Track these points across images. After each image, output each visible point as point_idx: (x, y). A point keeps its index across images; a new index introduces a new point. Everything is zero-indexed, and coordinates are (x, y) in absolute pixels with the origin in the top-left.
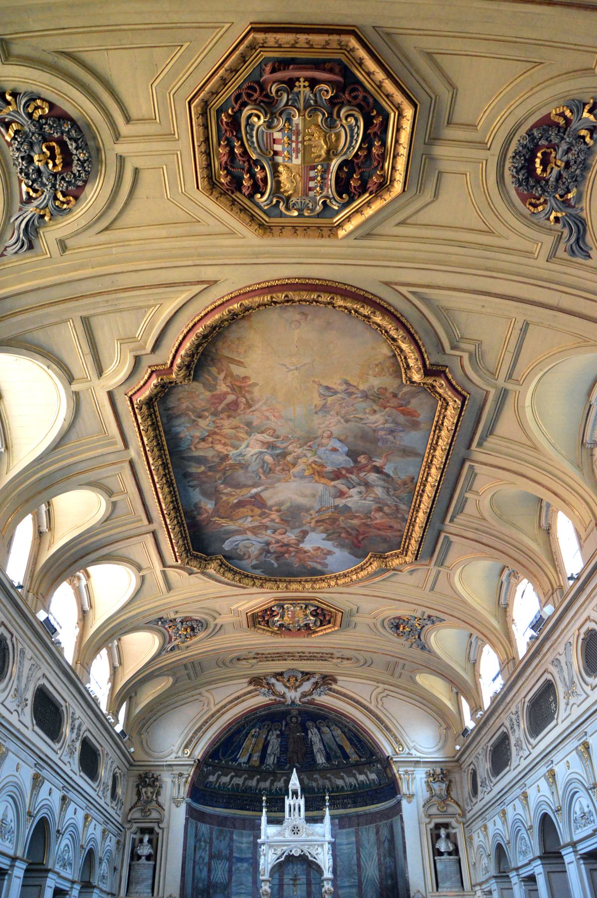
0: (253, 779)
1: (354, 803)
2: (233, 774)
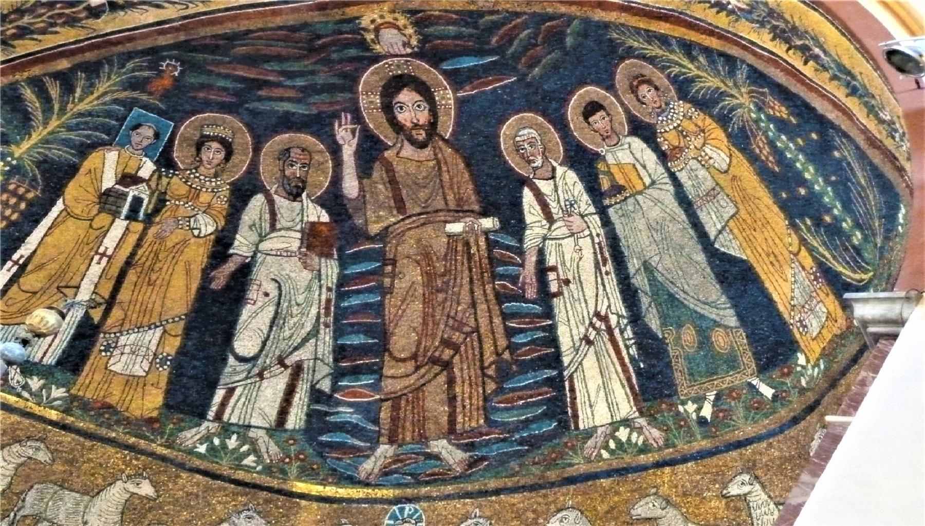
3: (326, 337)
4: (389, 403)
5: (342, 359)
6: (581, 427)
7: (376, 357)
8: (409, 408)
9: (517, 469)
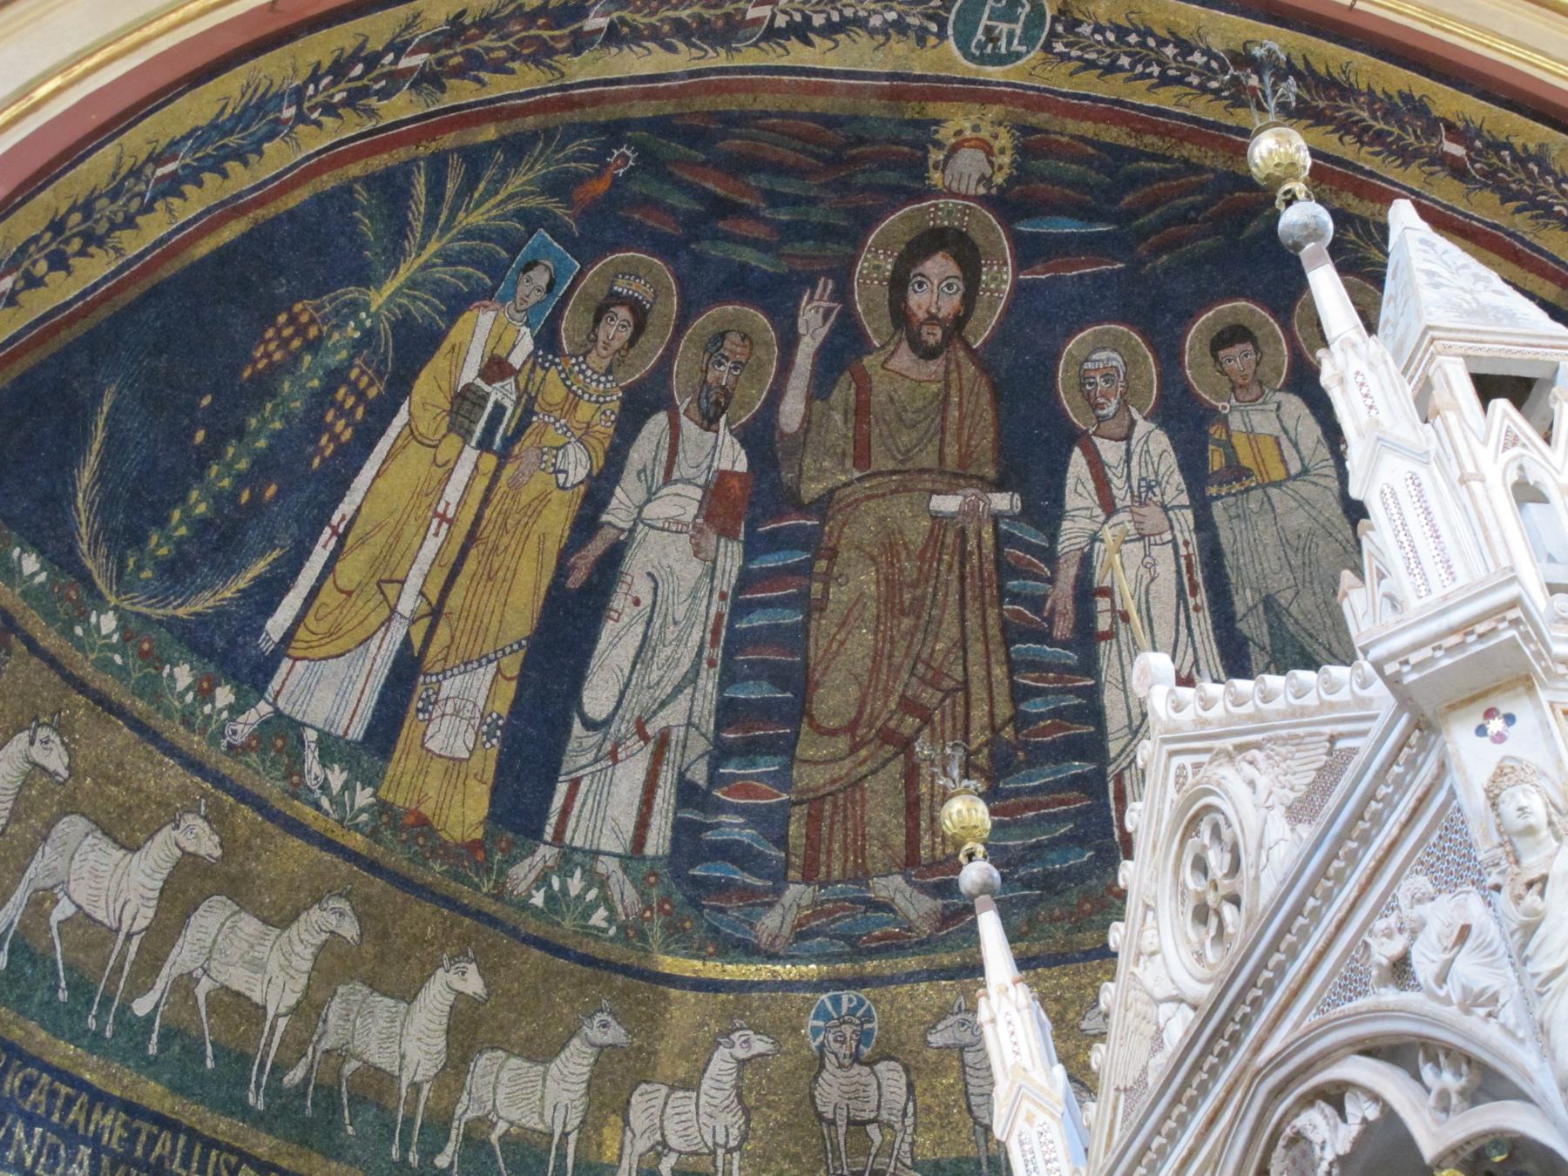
0: (408, 994)
2: (201, 839)
3: (709, 682)
4: (805, 808)
5: (729, 725)
7: (788, 726)
8: (839, 818)
9: (1025, 929)
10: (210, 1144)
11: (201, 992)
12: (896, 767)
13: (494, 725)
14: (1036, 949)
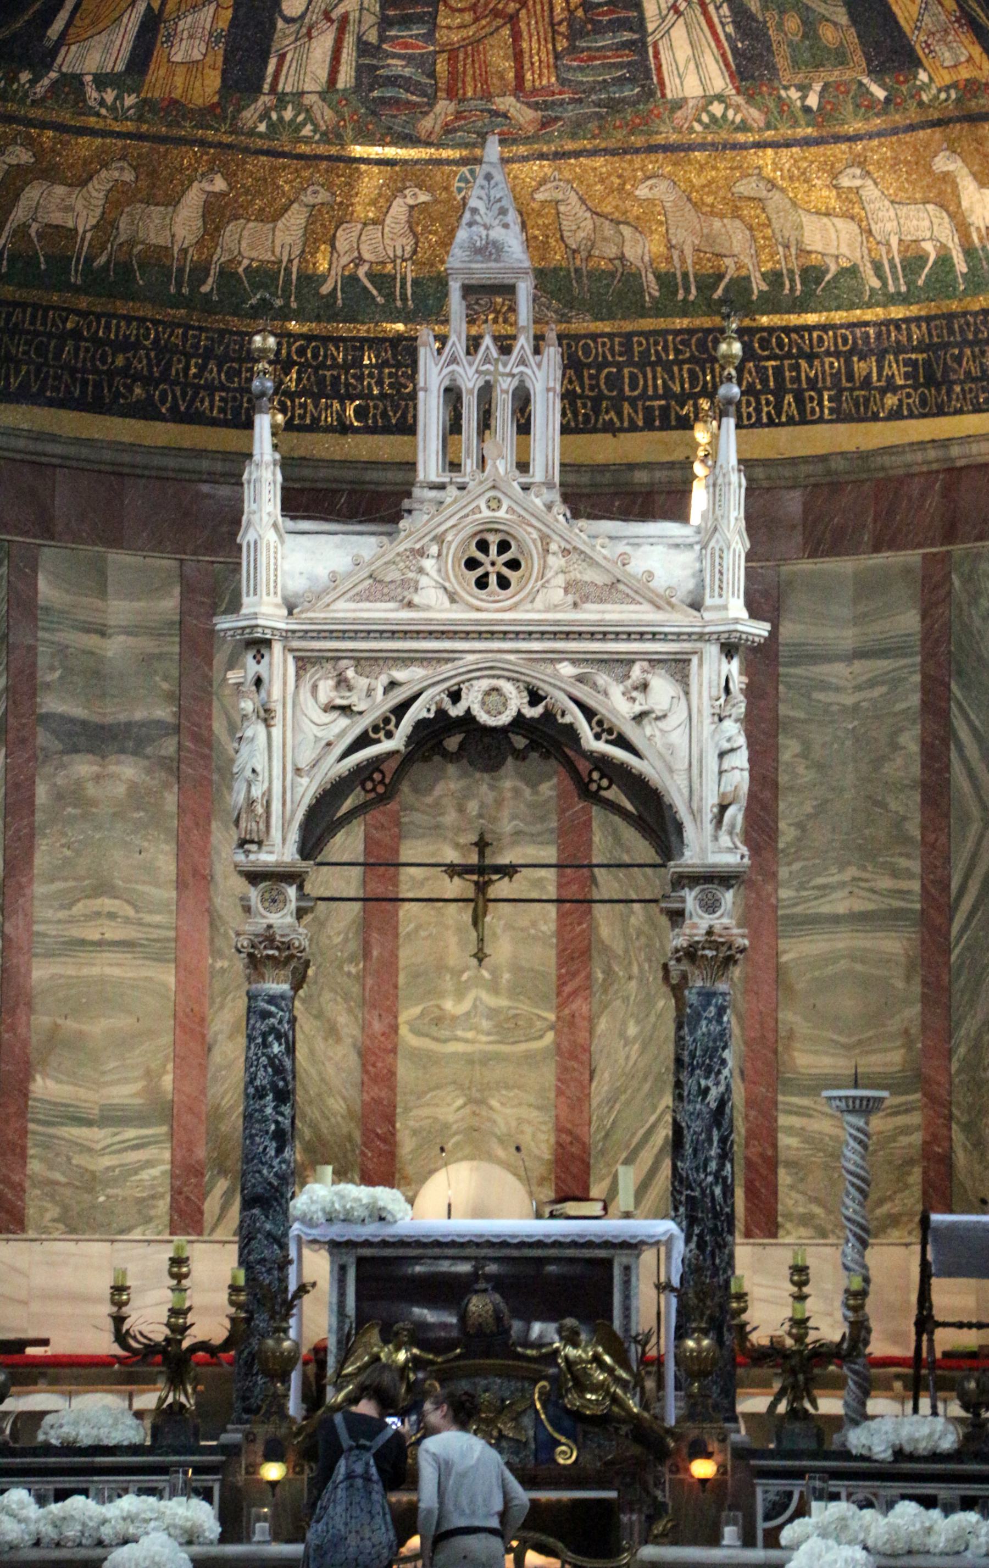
0: (173, 201)
1: (930, 381)
2: (23, 156)
4: (445, 55)
6: (669, 96)
7: (428, 5)
10: (46, 309)
11: (33, 232)
12: (506, 31)
13: (220, 35)
14: (603, 145)
